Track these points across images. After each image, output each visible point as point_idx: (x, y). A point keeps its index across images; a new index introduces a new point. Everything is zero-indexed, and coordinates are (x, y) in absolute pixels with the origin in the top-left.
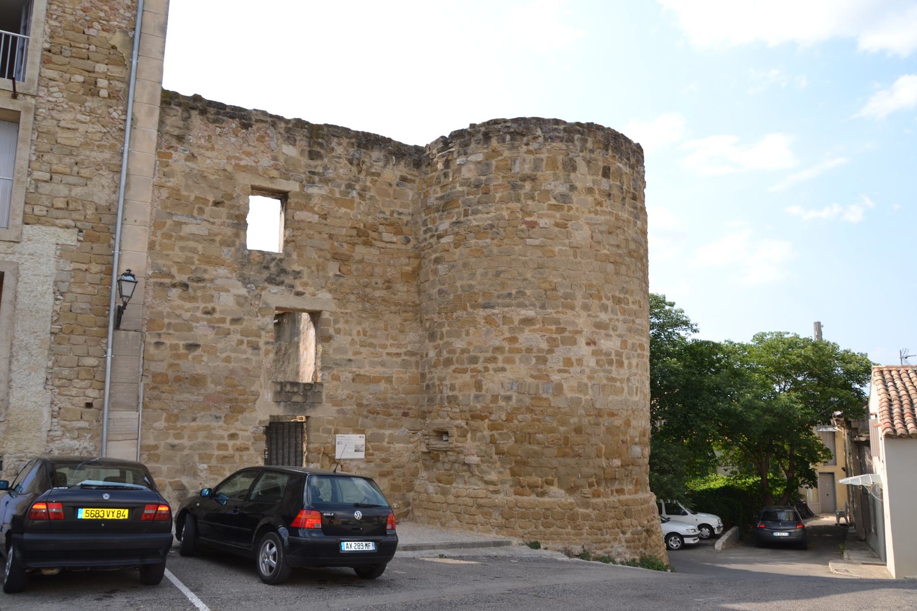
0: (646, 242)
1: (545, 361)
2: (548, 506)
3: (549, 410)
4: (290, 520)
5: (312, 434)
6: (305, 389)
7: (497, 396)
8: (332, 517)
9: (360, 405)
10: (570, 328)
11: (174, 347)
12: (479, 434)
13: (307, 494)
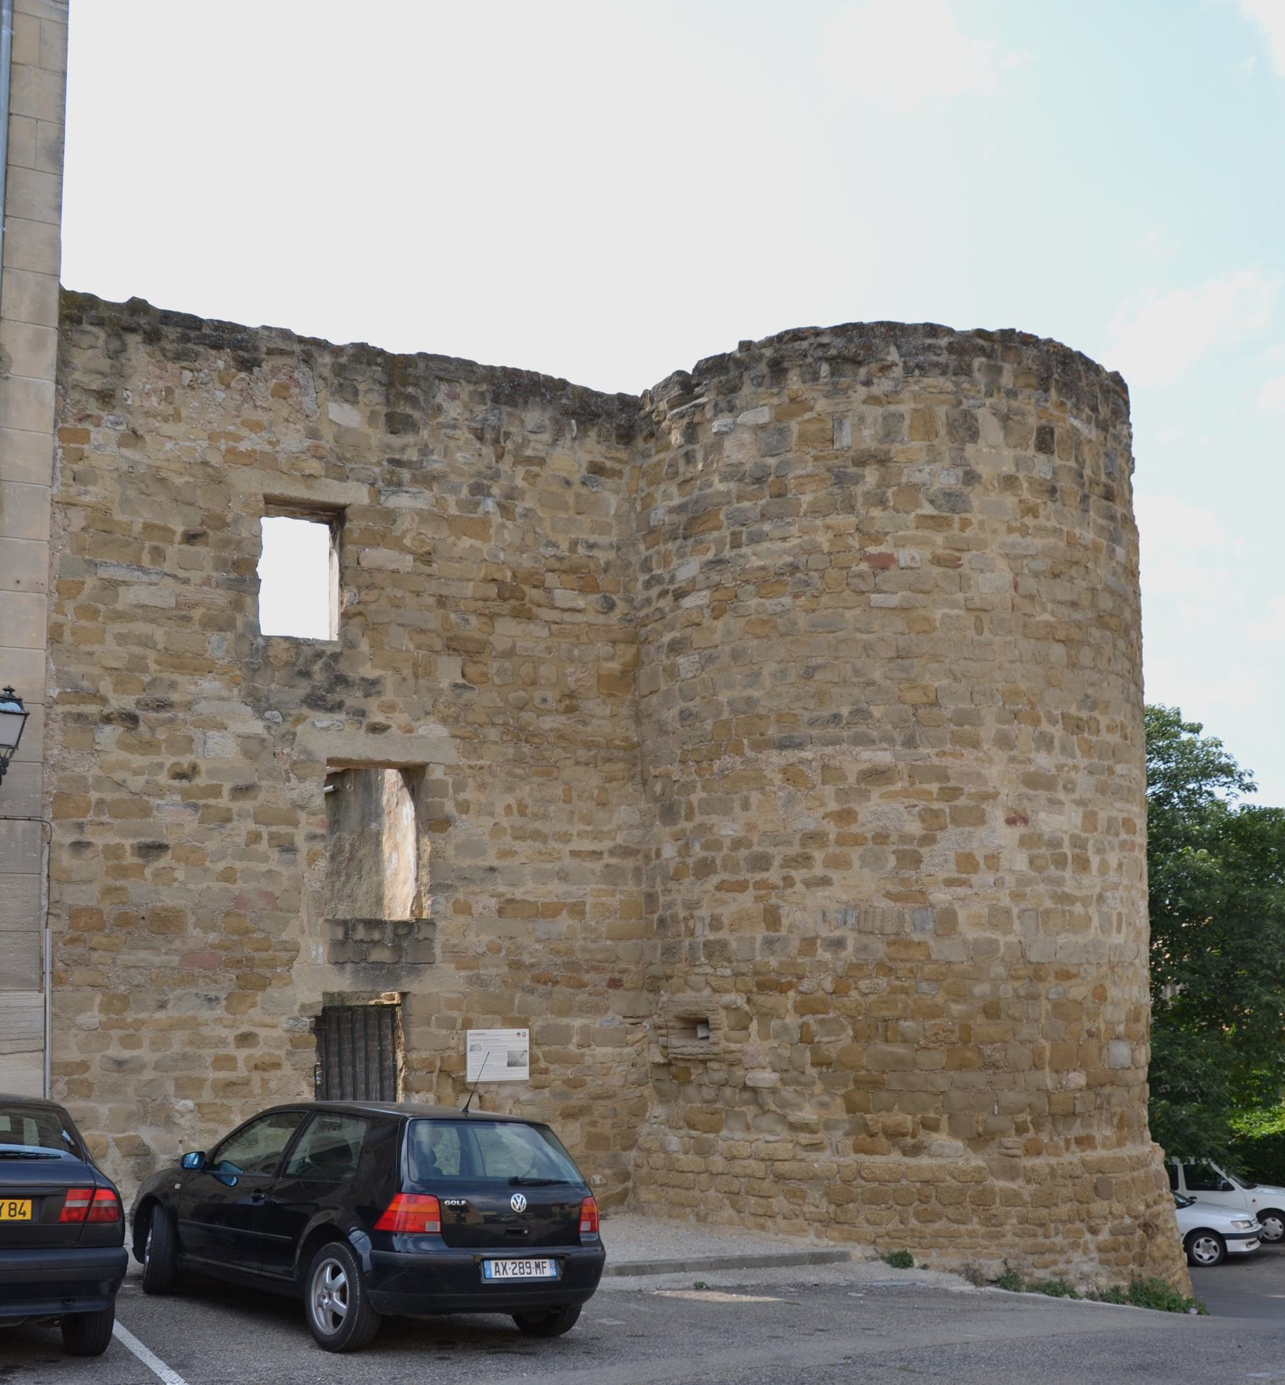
0: (1137, 594)
1: (917, 861)
2: (928, 1176)
3: (926, 968)
4: (372, 1216)
5: (416, 1031)
6: (397, 935)
7: (814, 939)
8: (463, 1209)
9: (516, 965)
10: (970, 788)
11: (113, 852)
12: (775, 1024)
13: (409, 1170)
